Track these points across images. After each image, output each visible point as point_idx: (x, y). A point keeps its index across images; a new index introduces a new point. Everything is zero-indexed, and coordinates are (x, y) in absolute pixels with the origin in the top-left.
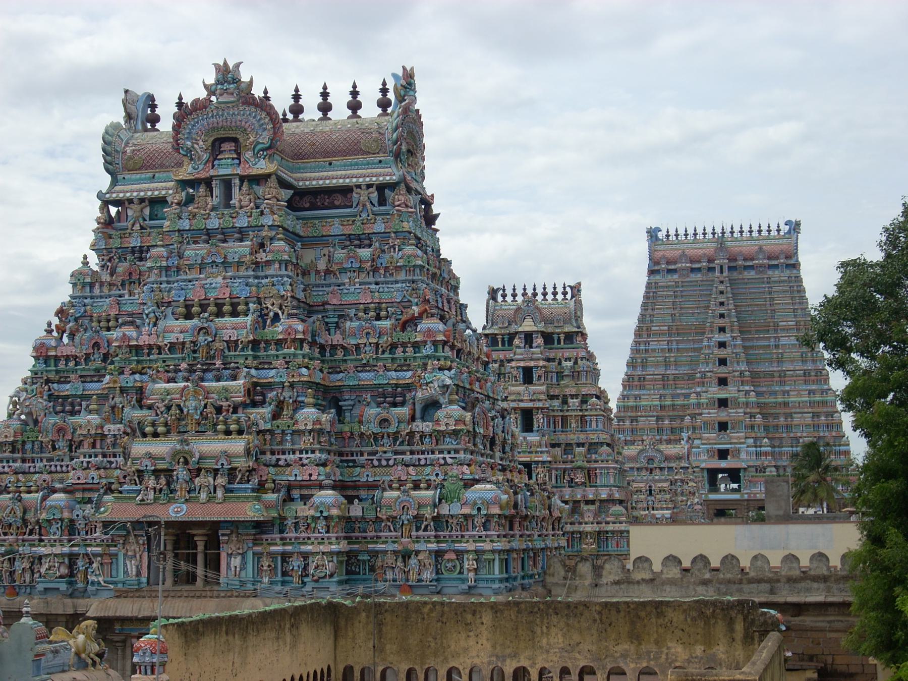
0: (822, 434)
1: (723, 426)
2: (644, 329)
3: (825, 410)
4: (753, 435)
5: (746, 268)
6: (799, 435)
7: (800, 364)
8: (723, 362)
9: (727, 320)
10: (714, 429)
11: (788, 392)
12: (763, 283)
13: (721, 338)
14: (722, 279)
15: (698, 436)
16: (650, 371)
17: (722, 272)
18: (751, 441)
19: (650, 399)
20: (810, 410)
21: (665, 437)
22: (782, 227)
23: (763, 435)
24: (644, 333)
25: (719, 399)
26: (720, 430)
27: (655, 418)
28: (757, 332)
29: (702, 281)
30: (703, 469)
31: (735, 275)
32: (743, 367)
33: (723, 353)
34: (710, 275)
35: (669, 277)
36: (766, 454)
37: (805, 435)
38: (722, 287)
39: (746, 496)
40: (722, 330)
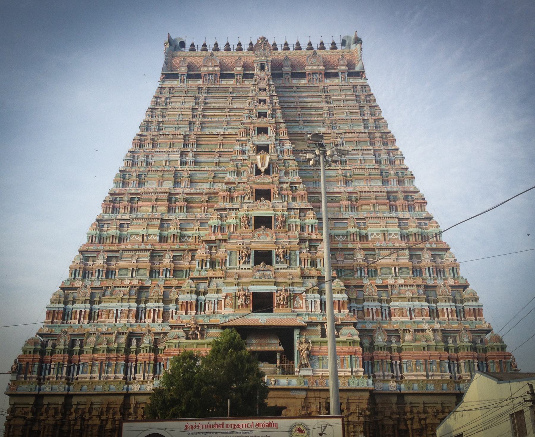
1: (263, 257)
3: (428, 246)
6: (391, 281)
7: (379, 183)
13: (262, 140)
15: (220, 274)
20: (403, 245)
22: (338, 45)
24: (148, 143)
26: (256, 263)
29: (234, 88)
31: (280, 82)
37: (401, 281)
38: (263, 84)
40: (263, 131)
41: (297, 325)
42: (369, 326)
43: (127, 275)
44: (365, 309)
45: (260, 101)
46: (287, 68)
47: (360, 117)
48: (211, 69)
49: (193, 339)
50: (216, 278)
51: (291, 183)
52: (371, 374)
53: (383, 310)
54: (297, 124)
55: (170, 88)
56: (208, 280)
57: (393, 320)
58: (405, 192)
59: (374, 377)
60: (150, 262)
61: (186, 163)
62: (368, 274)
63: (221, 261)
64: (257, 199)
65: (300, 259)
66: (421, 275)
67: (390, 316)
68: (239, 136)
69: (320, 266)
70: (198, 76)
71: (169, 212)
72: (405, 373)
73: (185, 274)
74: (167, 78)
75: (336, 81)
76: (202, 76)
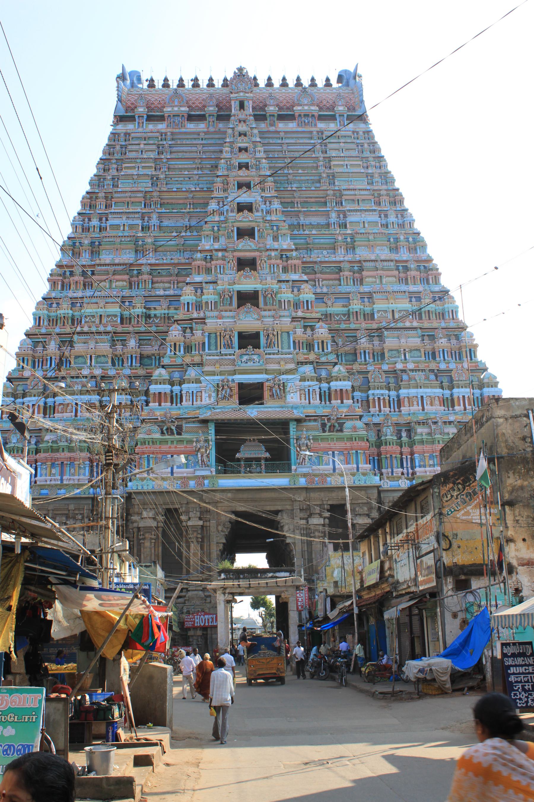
0: (443, 366)
1: (249, 340)
2: (101, 195)
3: (443, 325)
4: (312, 357)
5: (281, 118)
6: (399, 366)
7: (387, 251)
8: (246, 233)
9: (253, 172)
10: (229, 346)
11: (370, 296)
12: (311, 138)
13: (245, 197)
14: (242, 115)
15: (197, 359)
16: (106, 258)
17: (242, 106)
18: (308, 369)
19: (102, 307)
20: (415, 324)
21: (127, 372)
23: (332, 358)
24: (101, 204)
25: (239, 293)
27: (109, 337)
28: (305, 203)
29: (206, 133)
30: (205, 422)
31: (263, 125)
32: (286, 243)
33: (245, 220)
34: (221, 125)
35: (151, 127)
36: (341, 394)
37: (411, 366)
38: (242, 128)
39: (302, 482)
41: (294, 417)
42: (376, 420)
43: (85, 363)
44: (371, 398)
45: (240, 150)
46: (272, 108)
47: (362, 171)
48: (176, 109)
49: (170, 435)
50: (194, 365)
51: (282, 250)
52: (377, 471)
53: (391, 399)
54: (285, 178)
55: (126, 134)
56: (183, 368)
57: (403, 412)
58: (417, 261)
59: (382, 474)
60: (111, 347)
61: (149, 228)
62: (374, 358)
63: (197, 345)
64: (239, 270)
65: (294, 342)
66: (434, 357)
67: (399, 406)
68: (215, 192)
69: (318, 349)
70: (161, 118)
71: (131, 288)
72: (417, 469)
73: (154, 362)
74: (121, 121)
75: (332, 126)
76: (166, 118)
